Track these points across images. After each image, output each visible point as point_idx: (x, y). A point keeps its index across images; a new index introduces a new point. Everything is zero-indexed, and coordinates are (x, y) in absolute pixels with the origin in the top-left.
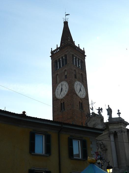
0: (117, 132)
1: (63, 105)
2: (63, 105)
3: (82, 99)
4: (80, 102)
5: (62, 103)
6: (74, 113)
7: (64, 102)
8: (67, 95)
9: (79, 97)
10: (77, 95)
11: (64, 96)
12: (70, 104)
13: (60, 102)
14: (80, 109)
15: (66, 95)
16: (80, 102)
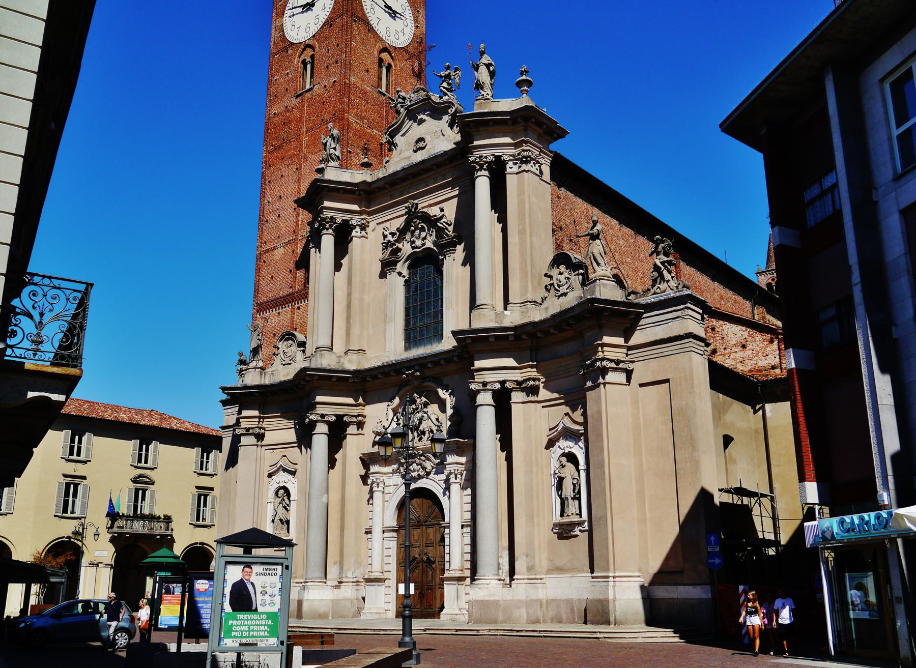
0: (504, 158)
1: (309, 66)
2: (309, 66)
3: (392, 50)
4: (381, 61)
5: (305, 60)
6: (346, 100)
7: (312, 57)
8: (329, 23)
9: (382, 40)
10: (371, 29)
11: (314, 29)
12: (337, 62)
13: (300, 57)
14: (380, 85)
15: (324, 24)
16: (381, 61)
